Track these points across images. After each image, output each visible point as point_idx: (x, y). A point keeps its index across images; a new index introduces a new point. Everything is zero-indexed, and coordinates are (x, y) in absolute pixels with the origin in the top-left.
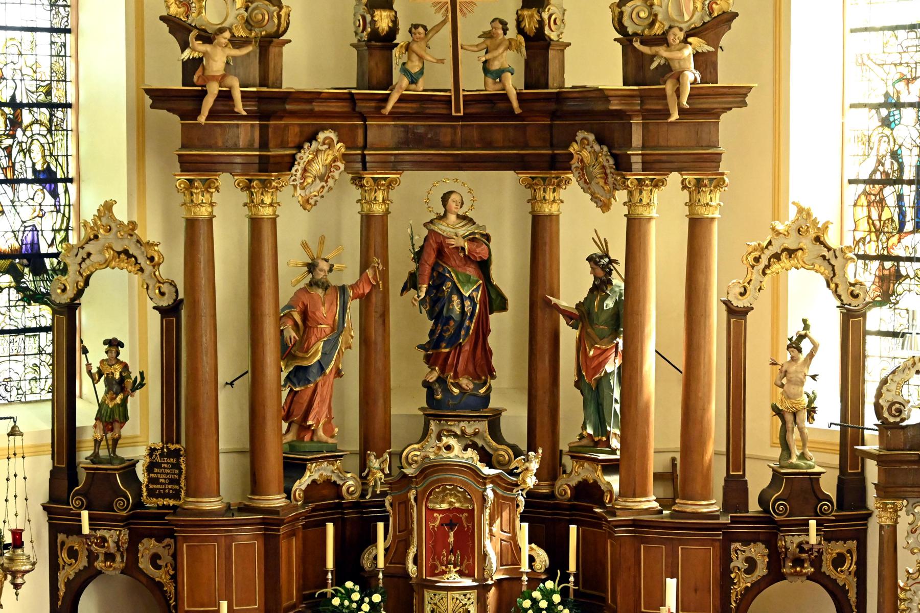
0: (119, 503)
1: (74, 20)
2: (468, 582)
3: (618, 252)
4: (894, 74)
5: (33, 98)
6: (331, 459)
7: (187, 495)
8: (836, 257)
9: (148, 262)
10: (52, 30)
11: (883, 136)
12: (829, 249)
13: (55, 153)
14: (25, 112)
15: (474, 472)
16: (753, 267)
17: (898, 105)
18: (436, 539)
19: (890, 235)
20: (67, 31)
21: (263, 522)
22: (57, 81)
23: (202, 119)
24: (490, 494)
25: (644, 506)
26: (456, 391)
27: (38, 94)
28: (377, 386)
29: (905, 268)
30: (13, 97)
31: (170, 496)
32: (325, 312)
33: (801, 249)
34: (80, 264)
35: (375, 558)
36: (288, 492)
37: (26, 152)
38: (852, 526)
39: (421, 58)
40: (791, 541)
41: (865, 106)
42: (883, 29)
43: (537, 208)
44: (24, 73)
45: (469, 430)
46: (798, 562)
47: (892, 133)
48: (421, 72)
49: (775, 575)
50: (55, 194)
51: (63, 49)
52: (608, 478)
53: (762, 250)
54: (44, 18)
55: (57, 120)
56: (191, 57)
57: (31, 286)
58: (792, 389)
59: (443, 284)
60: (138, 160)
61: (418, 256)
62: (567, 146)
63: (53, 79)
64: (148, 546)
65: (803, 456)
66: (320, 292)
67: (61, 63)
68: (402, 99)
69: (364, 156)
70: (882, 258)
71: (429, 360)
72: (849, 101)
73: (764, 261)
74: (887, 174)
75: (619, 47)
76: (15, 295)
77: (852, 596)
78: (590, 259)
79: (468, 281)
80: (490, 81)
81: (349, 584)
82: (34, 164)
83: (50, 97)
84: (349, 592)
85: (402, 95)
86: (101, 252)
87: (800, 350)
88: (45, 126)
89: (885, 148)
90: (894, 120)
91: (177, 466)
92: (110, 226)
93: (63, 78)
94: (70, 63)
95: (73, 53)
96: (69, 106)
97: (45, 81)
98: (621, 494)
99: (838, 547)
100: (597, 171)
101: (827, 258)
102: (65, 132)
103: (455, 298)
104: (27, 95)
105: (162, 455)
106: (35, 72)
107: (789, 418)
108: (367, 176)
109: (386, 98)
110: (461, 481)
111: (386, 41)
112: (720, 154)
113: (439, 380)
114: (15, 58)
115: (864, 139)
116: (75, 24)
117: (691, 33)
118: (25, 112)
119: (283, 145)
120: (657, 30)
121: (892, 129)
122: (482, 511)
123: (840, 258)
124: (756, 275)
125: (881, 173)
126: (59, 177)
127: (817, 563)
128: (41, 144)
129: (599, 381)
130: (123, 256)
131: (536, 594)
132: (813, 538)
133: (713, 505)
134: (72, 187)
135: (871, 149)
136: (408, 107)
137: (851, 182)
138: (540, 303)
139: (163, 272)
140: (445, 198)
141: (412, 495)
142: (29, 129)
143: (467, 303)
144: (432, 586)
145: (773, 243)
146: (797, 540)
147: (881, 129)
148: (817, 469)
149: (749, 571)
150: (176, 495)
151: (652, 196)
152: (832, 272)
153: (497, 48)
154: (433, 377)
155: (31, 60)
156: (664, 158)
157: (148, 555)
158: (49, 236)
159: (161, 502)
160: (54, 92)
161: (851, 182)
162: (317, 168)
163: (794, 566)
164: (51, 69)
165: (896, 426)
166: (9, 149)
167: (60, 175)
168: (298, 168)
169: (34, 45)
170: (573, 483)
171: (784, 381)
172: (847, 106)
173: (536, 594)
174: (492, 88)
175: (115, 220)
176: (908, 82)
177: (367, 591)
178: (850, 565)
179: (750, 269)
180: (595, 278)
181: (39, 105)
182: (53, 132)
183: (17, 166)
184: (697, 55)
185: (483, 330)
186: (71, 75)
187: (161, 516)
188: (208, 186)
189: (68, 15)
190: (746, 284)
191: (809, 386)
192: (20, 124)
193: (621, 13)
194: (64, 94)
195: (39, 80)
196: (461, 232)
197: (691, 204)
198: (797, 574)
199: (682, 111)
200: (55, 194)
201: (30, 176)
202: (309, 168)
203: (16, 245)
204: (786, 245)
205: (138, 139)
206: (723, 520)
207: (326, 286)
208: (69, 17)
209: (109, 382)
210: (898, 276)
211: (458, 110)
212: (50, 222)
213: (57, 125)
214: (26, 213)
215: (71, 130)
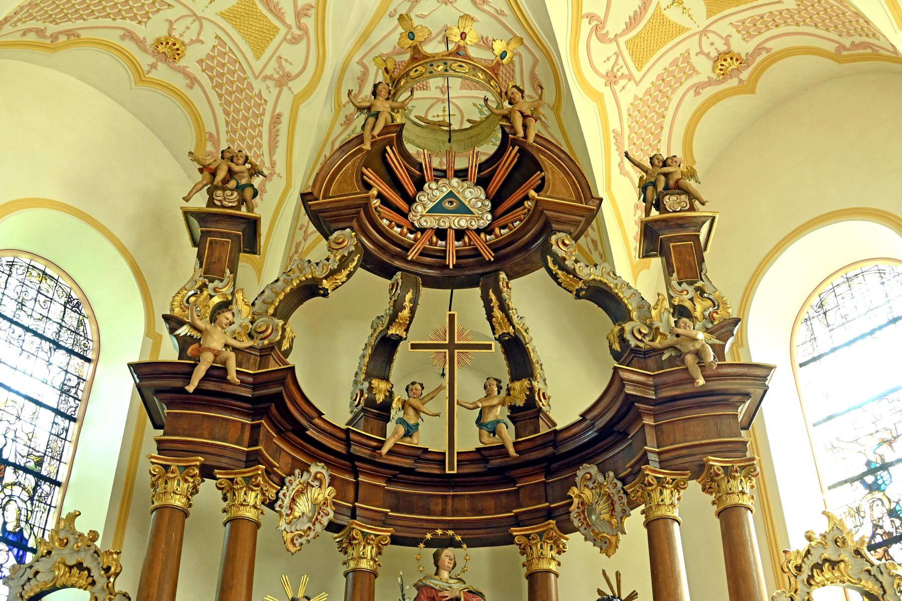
1: (82, 411)
8: (882, 573)
9: (103, 572)
10: (57, 412)
11: (874, 501)
12: (872, 565)
13: (31, 521)
16: (796, 577)
17: (885, 467)
20: (72, 419)
22: (51, 457)
27: (28, 460)
33: (842, 561)
41: (846, 482)
44: (17, 436)
47: (884, 494)
51: (65, 433)
54: (52, 398)
55: (42, 493)
56: (188, 334)
60: (118, 528)
63: (47, 453)
67: (60, 444)
69: (354, 509)
74: (890, 534)
82: (5, 523)
83: (40, 468)
85: (425, 248)
88: (27, 492)
89: (880, 511)
90: (884, 482)
92: (67, 540)
93: (58, 458)
95: (74, 438)
96: (59, 484)
97: (39, 452)
101: (872, 574)
102: (48, 507)
104: (16, 455)
106: (30, 440)
112: (745, 443)
114: (13, 419)
115: (852, 512)
116: (81, 414)
118: (9, 470)
121: (883, 491)
123: (885, 575)
125: (882, 535)
126: (30, 545)
128: (19, 508)
130: (75, 571)
135: (863, 518)
142: (9, 487)
145: (812, 551)
147: (870, 496)
151: (673, 498)
152: (882, 589)
156: (685, 452)
160: (45, 465)
164: (48, 445)
167: (31, 544)
169: (36, 417)
172: (825, 488)
175: (74, 533)
176: (889, 442)
179: (792, 579)
181: (26, 470)
182: (35, 502)
186: (67, 457)
189: (77, 407)
190: (792, 593)
194: (55, 471)
195: (32, 449)
202: (298, 500)
204: (826, 555)
205: (122, 508)
208: (77, 409)
211: (451, 468)
213: (41, 496)
215: (55, 507)
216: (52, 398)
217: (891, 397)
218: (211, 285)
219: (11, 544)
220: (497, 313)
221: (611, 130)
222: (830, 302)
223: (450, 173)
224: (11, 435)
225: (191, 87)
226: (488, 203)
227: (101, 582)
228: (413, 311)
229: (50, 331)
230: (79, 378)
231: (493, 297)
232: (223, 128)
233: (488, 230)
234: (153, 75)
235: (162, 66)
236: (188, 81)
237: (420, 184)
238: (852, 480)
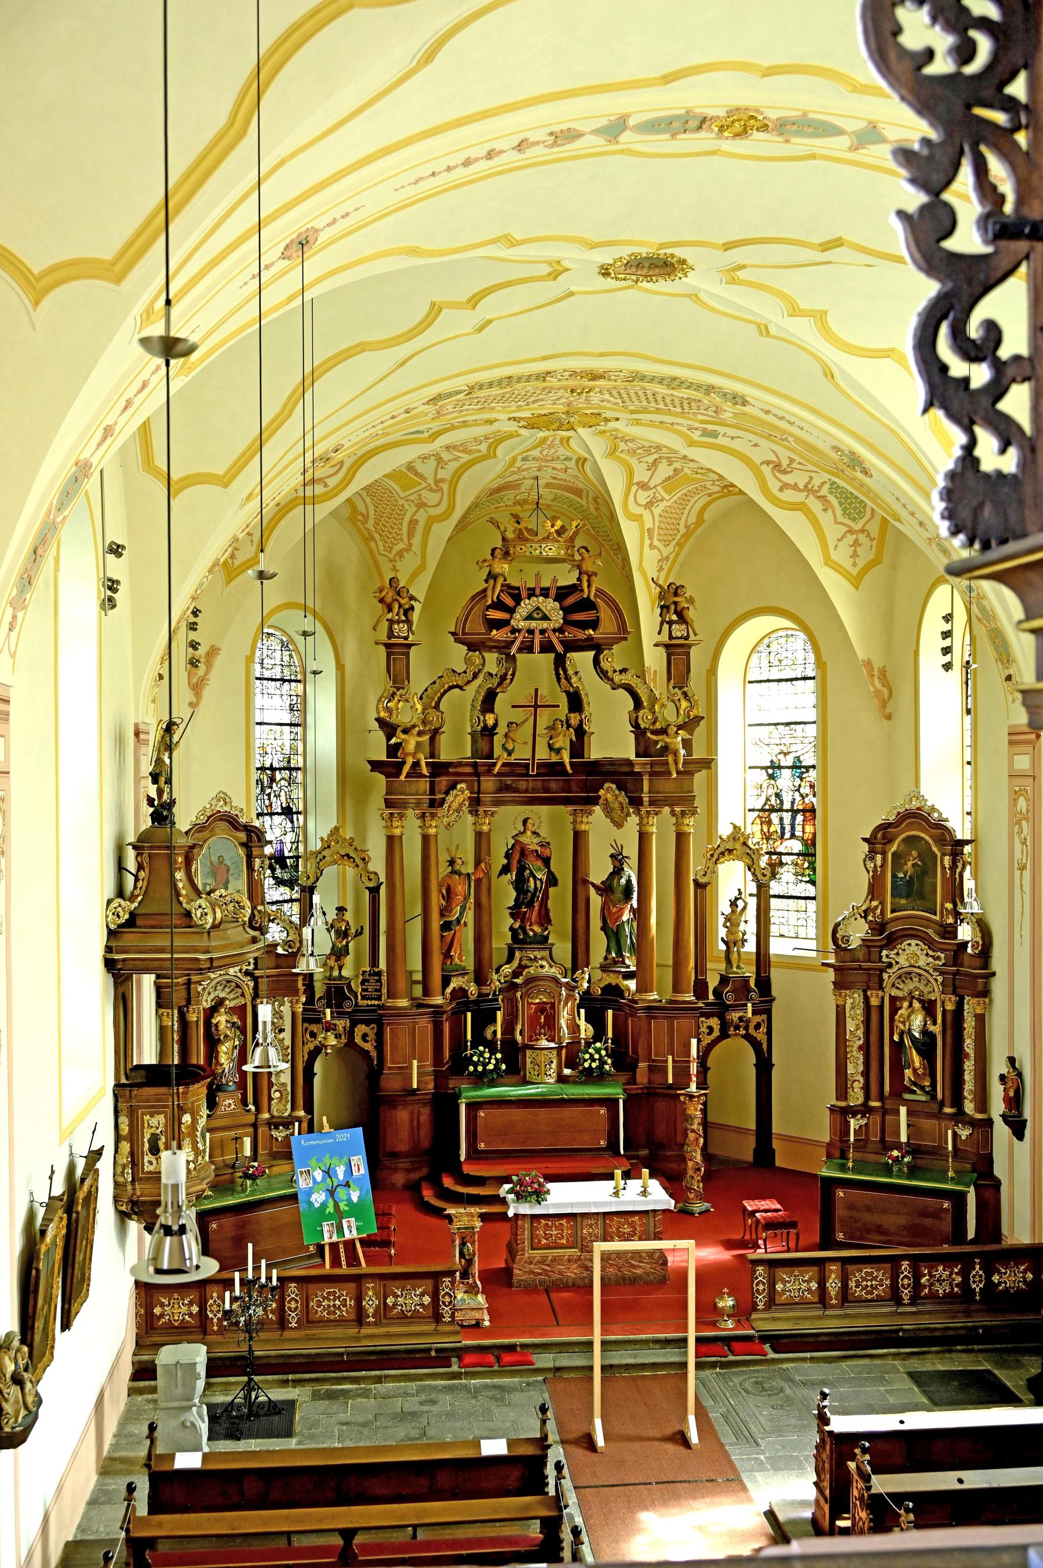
0: (347, 1003)
2: (553, 1045)
3: (632, 851)
4: (777, 750)
5: (282, 765)
6: (463, 975)
7: (389, 997)
10: (291, 725)
14: (277, 772)
15: (555, 980)
17: (780, 767)
18: (533, 1021)
19: (775, 840)
20: (298, 725)
21: (433, 1013)
23: (402, 778)
24: (564, 993)
25: (652, 998)
26: (531, 934)
28: (485, 930)
29: (785, 859)
31: (375, 999)
32: (460, 888)
35: (495, 1032)
36: (443, 994)
37: (278, 796)
38: (764, 1006)
39: (514, 741)
40: (735, 1016)
42: (769, 724)
43: (578, 827)
45: (539, 956)
46: (737, 1028)
48: (513, 750)
49: (724, 1035)
50: (292, 822)
52: (626, 982)
53: (715, 850)
54: (286, 718)
57: (280, 876)
58: (734, 929)
59: (524, 871)
61: (508, 856)
62: (597, 792)
64: (360, 1029)
65: (738, 967)
66: (457, 877)
68: (504, 765)
70: (770, 853)
71: (512, 915)
72: (748, 765)
73: (716, 857)
75: (633, 736)
76: (272, 881)
77: (765, 1047)
78: (612, 856)
79: (540, 870)
80: (553, 754)
81: (481, 1048)
84: (481, 1054)
86: (332, 856)
87: (737, 906)
91: (379, 981)
94: (300, 745)
98: (639, 990)
99: (758, 1018)
100: (616, 805)
103: (531, 879)
105: (370, 975)
107: (732, 945)
108: (481, 809)
109: (494, 764)
110: (551, 987)
111: (489, 732)
113: (520, 927)
114: (273, 741)
117: (680, 727)
119: (440, 793)
120: (658, 726)
122: (559, 1003)
124: (711, 864)
127: (746, 1028)
129: (618, 926)
131: (591, 1051)
132: (750, 1014)
133: (690, 997)
134: (301, 817)
136: (506, 769)
137: (750, 810)
138: (580, 882)
139: (371, 867)
140: (525, 822)
141: (519, 994)
143: (538, 882)
144: (532, 1048)
146: (738, 1015)
148: (747, 974)
149: (709, 1034)
150: (379, 998)
153: (559, 735)
154: (517, 925)
155: (280, 743)
157: (360, 1034)
158: (289, 846)
159: (369, 1002)
161: (750, 810)
162: (455, 805)
163: (735, 1030)
165: (845, 949)
166: (269, 795)
168: (446, 805)
170: (602, 985)
171: (728, 924)
173: (591, 1051)
174: (554, 759)
176: (785, 754)
177: (493, 1052)
178: (763, 1029)
180: (614, 867)
181: (284, 769)
184: (683, 740)
185: (546, 896)
187: (375, 1011)
188: (401, 816)
191: (742, 927)
193: (637, 717)
196: (535, 841)
197: (677, 824)
198: (736, 1035)
199: (678, 772)
200: (292, 822)
201: (280, 811)
206: (700, 1004)
207: (460, 874)
209: (338, 933)
210: (781, 864)
212: (290, 837)
217: (792, 726)
218: (398, 693)
220: (563, 681)
221: (646, 527)
222: (774, 647)
223: (538, 591)
226: (561, 612)
227: (361, 864)
228: (512, 680)
229: (277, 673)
231: (561, 672)
232: (372, 509)
233: (561, 630)
237: (518, 599)
238: (762, 768)
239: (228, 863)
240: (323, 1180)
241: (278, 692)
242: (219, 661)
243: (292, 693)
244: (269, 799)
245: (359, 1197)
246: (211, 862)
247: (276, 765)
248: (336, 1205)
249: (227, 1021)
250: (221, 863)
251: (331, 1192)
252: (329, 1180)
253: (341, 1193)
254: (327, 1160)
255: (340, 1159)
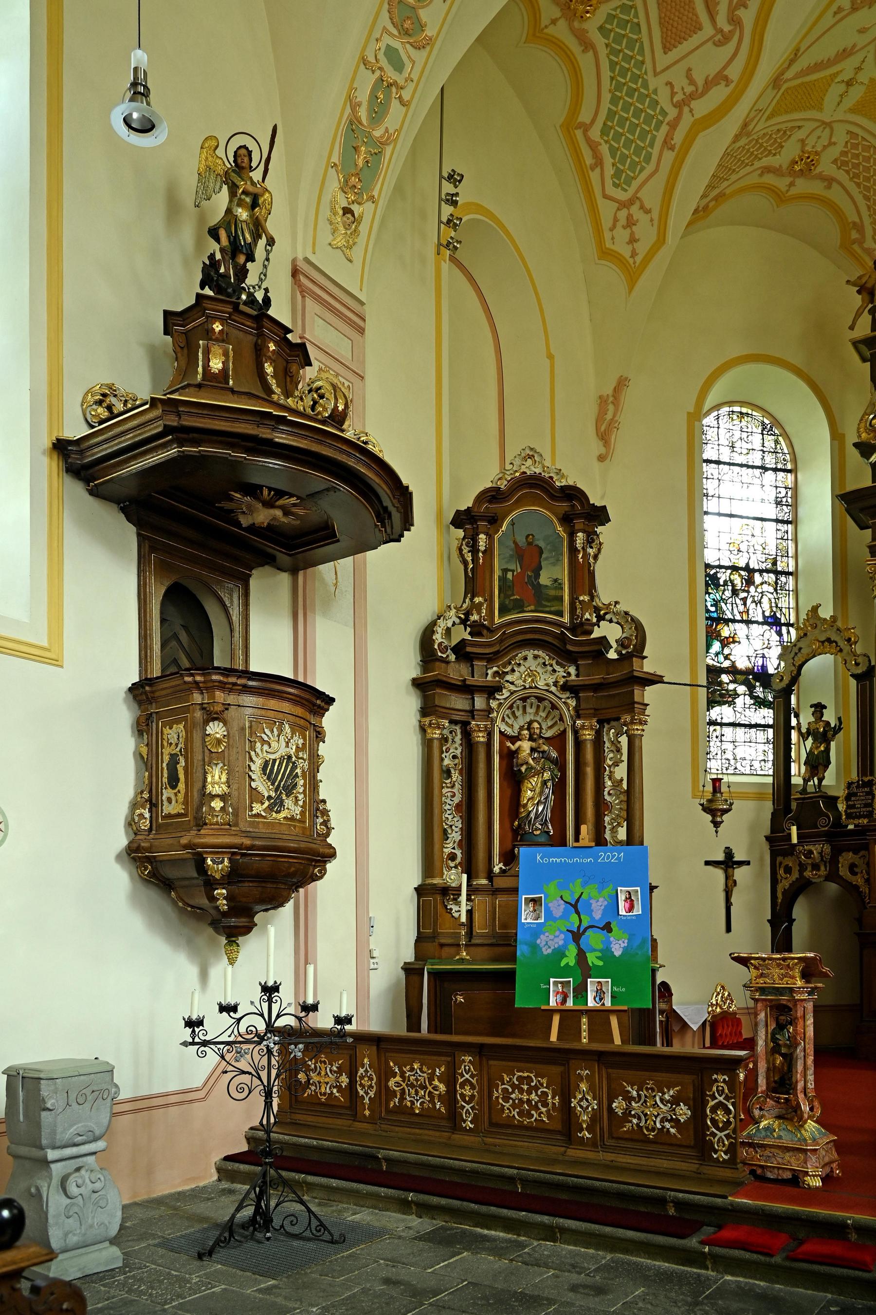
5: (763, 566)
10: (777, 521)
13: (779, 605)
14: (757, 575)
20: (787, 522)
30: (748, 565)
34: (793, 658)
54: (771, 512)
76: (749, 701)
82: (763, 612)
94: (791, 545)
118: (757, 575)
155: (762, 541)
160: (779, 563)
166: (744, 600)
181: (768, 571)
183: (751, 612)
192: (753, 583)
200: (779, 634)
201: (761, 619)
203: (750, 666)
214: (758, 644)
216: (771, 512)
219: (770, 624)
224: (751, 550)
225: (829, 187)
229: (756, 459)
230: (786, 488)
234: (793, 191)
235: (800, 182)
236: (826, 184)
239: (542, 544)
240: (565, 916)
241: (758, 481)
242: (630, 397)
243: (780, 484)
244: (745, 604)
245: (625, 949)
246: (515, 542)
247: (753, 565)
248: (581, 956)
249: (533, 750)
250: (530, 544)
251: (577, 936)
252: (574, 918)
253: (593, 939)
254: (577, 888)
255: (600, 890)
